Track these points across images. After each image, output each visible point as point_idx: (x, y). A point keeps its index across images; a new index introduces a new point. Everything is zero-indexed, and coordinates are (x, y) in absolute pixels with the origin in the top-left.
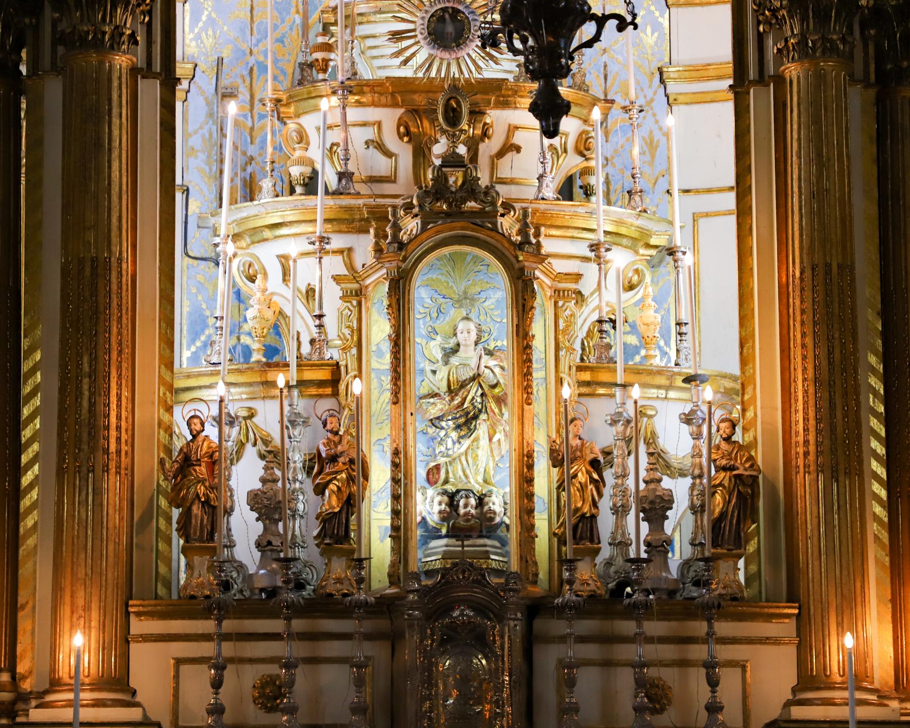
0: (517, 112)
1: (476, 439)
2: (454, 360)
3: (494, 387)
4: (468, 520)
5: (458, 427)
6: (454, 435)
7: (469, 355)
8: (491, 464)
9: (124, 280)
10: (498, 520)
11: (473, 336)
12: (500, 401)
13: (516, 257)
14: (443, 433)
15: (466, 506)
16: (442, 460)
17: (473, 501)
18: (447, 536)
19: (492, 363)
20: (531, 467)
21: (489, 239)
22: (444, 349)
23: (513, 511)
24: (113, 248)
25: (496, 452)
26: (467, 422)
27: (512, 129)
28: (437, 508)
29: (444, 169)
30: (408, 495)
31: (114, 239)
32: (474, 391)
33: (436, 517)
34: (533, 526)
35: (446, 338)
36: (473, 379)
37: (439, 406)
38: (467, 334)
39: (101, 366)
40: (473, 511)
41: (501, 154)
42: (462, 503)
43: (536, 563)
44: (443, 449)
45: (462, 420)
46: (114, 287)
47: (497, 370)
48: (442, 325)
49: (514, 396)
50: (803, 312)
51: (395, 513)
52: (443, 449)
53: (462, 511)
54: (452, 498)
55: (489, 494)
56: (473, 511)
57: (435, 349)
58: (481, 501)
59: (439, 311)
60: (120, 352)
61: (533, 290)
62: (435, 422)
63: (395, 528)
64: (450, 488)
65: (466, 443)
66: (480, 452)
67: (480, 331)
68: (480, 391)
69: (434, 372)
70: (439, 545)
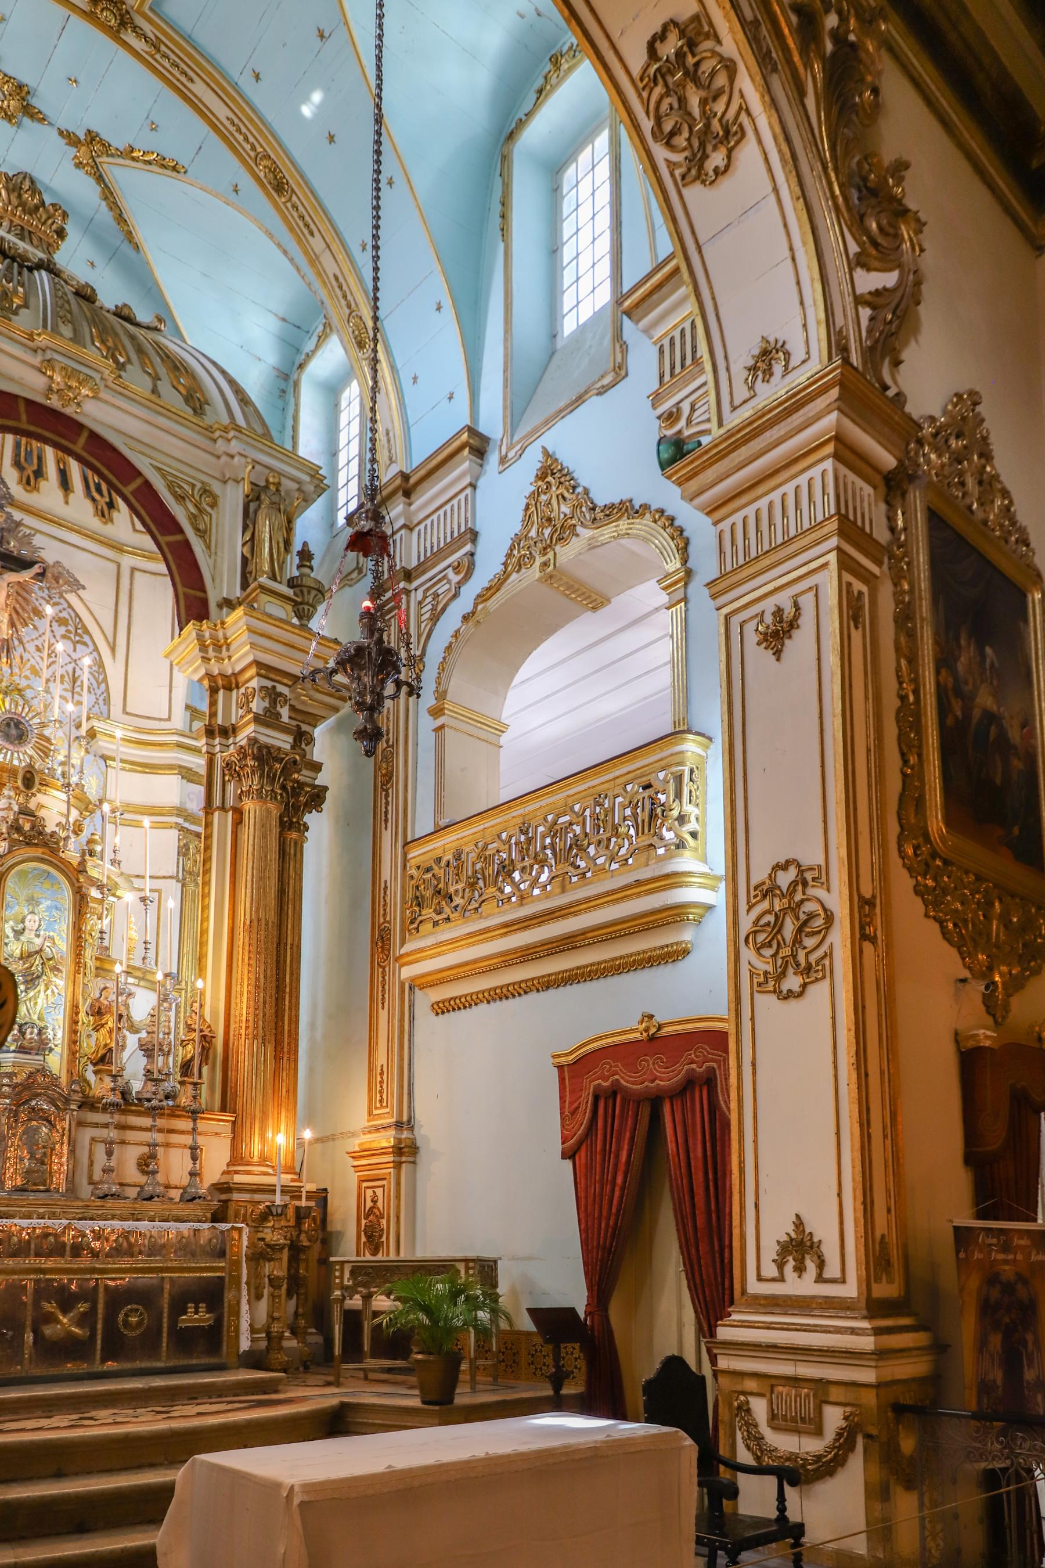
1: (39, 991)
3: (49, 959)
12: (55, 969)
15: (31, 1033)
17: (36, 1031)
18: (14, 1051)
22: (14, 930)
36: (37, 952)
38: (32, 922)
42: (28, 1031)
45: (29, 978)
49: (67, 966)
53: (28, 1036)
55: (46, 1027)
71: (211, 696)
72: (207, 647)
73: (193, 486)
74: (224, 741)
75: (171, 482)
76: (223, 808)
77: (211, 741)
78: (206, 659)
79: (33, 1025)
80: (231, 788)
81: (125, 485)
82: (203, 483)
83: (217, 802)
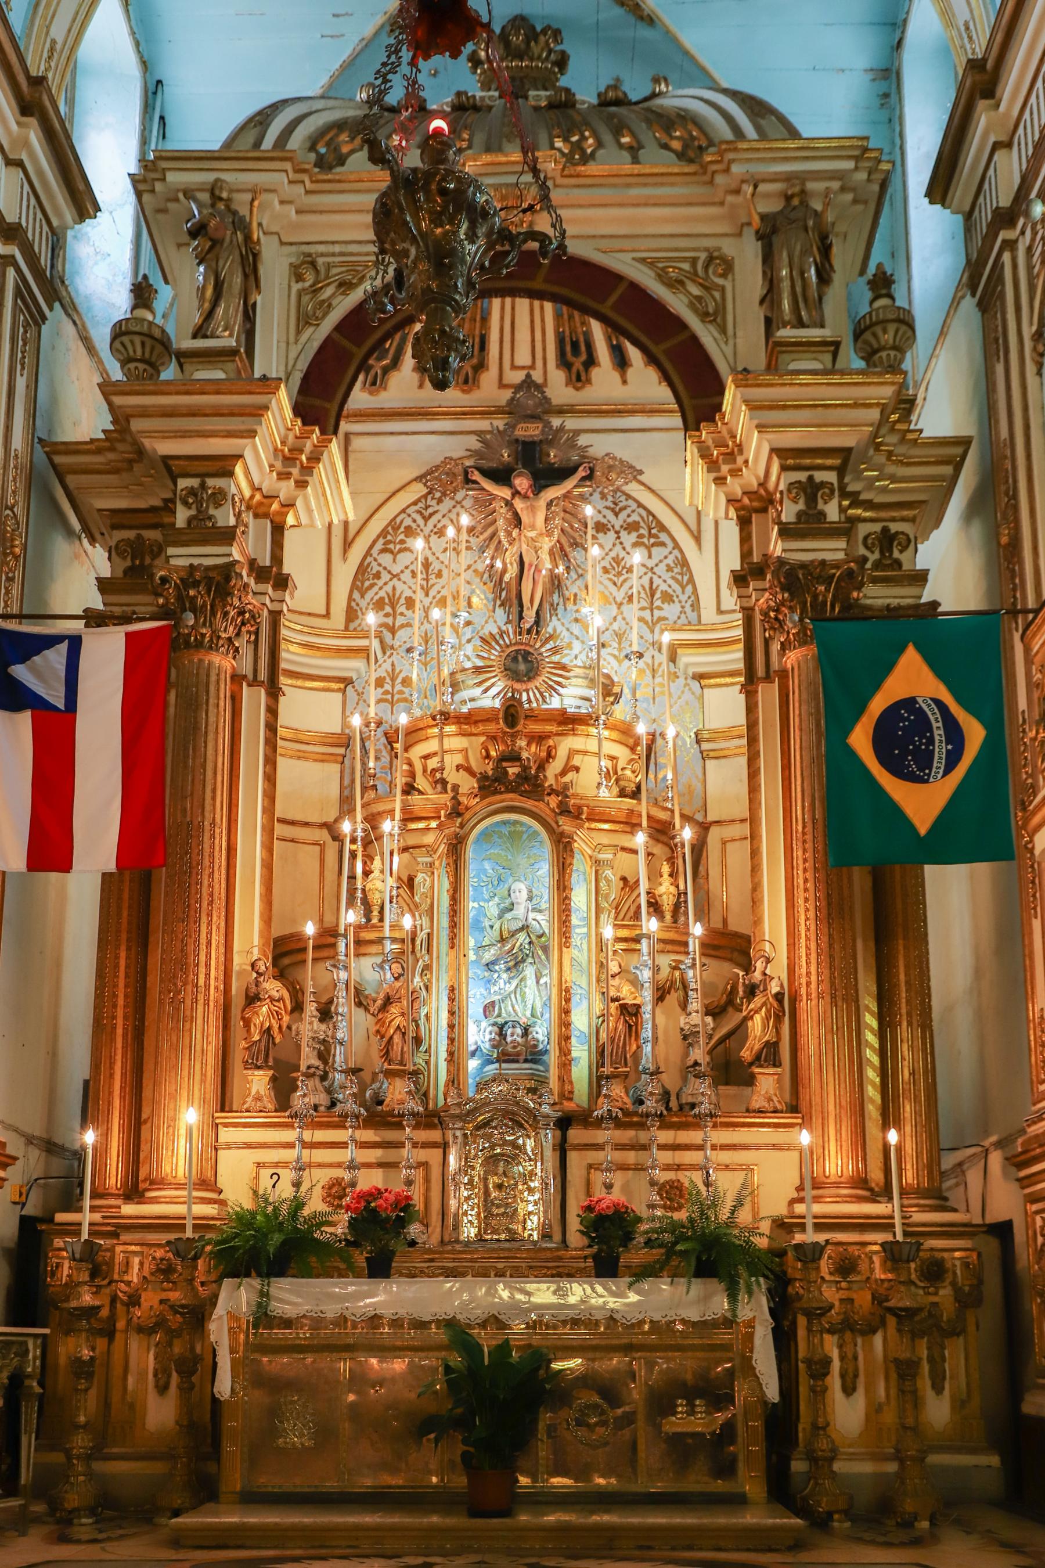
0: (576, 738)
2: (508, 916)
4: (515, 1047)
5: (509, 969)
6: (505, 976)
7: (520, 911)
8: (538, 1005)
9: (217, 842)
10: (541, 1047)
11: (524, 894)
13: (557, 823)
14: (496, 975)
16: (496, 998)
17: (519, 1031)
19: (539, 917)
20: (568, 1000)
21: (534, 809)
23: (554, 1038)
24: (207, 814)
25: (543, 993)
26: (516, 964)
27: (572, 753)
28: (488, 1037)
29: (504, 764)
30: (463, 1026)
31: (208, 807)
32: (522, 937)
33: (487, 1045)
34: (570, 1051)
35: (503, 899)
36: (522, 929)
37: (492, 951)
39: (192, 913)
40: (519, 1039)
41: (564, 773)
42: (509, 1032)
43: (571, 1082)
44: (496, 988)
45: (511, 964)
46: (206, 846)
47: (543, 923)
48: (502, 891)
50: (805, 861)
51: (451, 1040)
52: (496, 988)
53: (509, 1039)
54: (501, 1028)
56: (519, 1039)
57: (492, 909)
58: (526, 1032)
59: (500, 880)
60: (211, 903)
61: (572, 850)
62: (489, 966)
63: (451, 1054)
64: (500, 1021)
65: (515, 983)
66: (527, 990)
67: (530, 891)
68: (528, 940)
69: (492, 927)
70: (492, 1069)
71: (741, 530)
72: (716, 462)
73: (694, 261)
74: (760, 584)
75: (663, 269)
76: (768, 678)
77: (744, 591)
78: (720, 481)
79: (515, 1024)
80: (775, 647)
81: (603, 301)
82: (707, 250)
83: (760, 671)
